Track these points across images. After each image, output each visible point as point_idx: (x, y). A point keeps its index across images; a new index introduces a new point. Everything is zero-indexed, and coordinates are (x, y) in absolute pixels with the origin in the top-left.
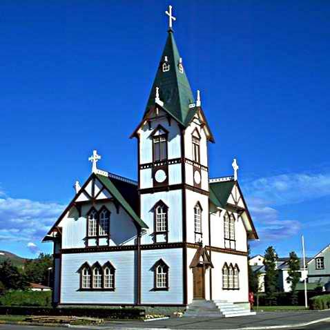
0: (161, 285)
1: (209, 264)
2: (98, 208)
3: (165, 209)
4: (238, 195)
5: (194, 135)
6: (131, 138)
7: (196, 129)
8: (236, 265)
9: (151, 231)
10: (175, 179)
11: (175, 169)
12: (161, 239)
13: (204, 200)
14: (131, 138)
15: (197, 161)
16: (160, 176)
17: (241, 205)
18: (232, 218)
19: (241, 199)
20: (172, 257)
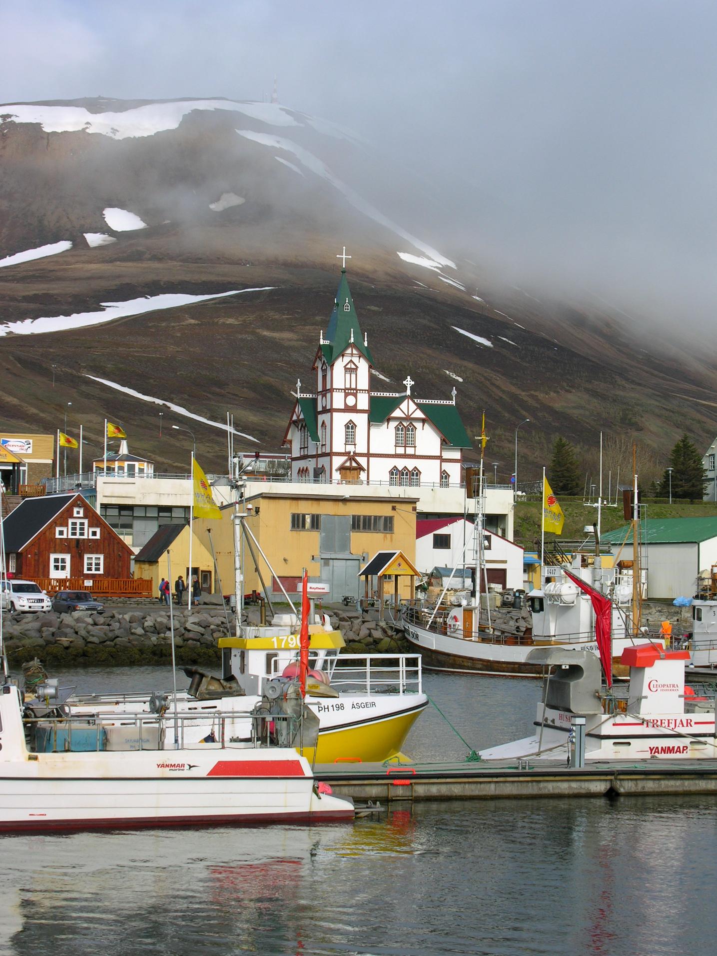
3: (354, 426)
13: (361, 420)
16: (351, 401)
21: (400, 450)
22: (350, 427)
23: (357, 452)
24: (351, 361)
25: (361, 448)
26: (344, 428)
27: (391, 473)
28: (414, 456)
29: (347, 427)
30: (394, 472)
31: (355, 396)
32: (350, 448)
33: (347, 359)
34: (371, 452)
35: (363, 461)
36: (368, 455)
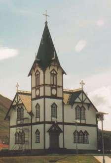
0: (38, 141)
1: (60, 131)
2: (20, 107)
4: (84, 97)
5: (53, 72)
6: (29, 76)
7: (54, 70)
8: (86, 131)
9: (35, 117)
10: (42, 94)
11: (42, 88)
12: (38, 120)
14: (29, 76)
15: (55, 84)
17: (87, 101)
18: (83, 109)
19: (87, 99)
20: (40, 127)
21: (78, 121)
22: (54, 106)
23: (58, 121)
24: (37, 71)
25: (60, 120)
26: (51, 107)
27: (74, 134)
28: (85, 125)
29: (52, 106)
30: (75, 133)
31: (56, 89)
32: (54, 119)
33: (52, 68)
34: (65, 121)
35: (61, 126)
36: (63, 123)
